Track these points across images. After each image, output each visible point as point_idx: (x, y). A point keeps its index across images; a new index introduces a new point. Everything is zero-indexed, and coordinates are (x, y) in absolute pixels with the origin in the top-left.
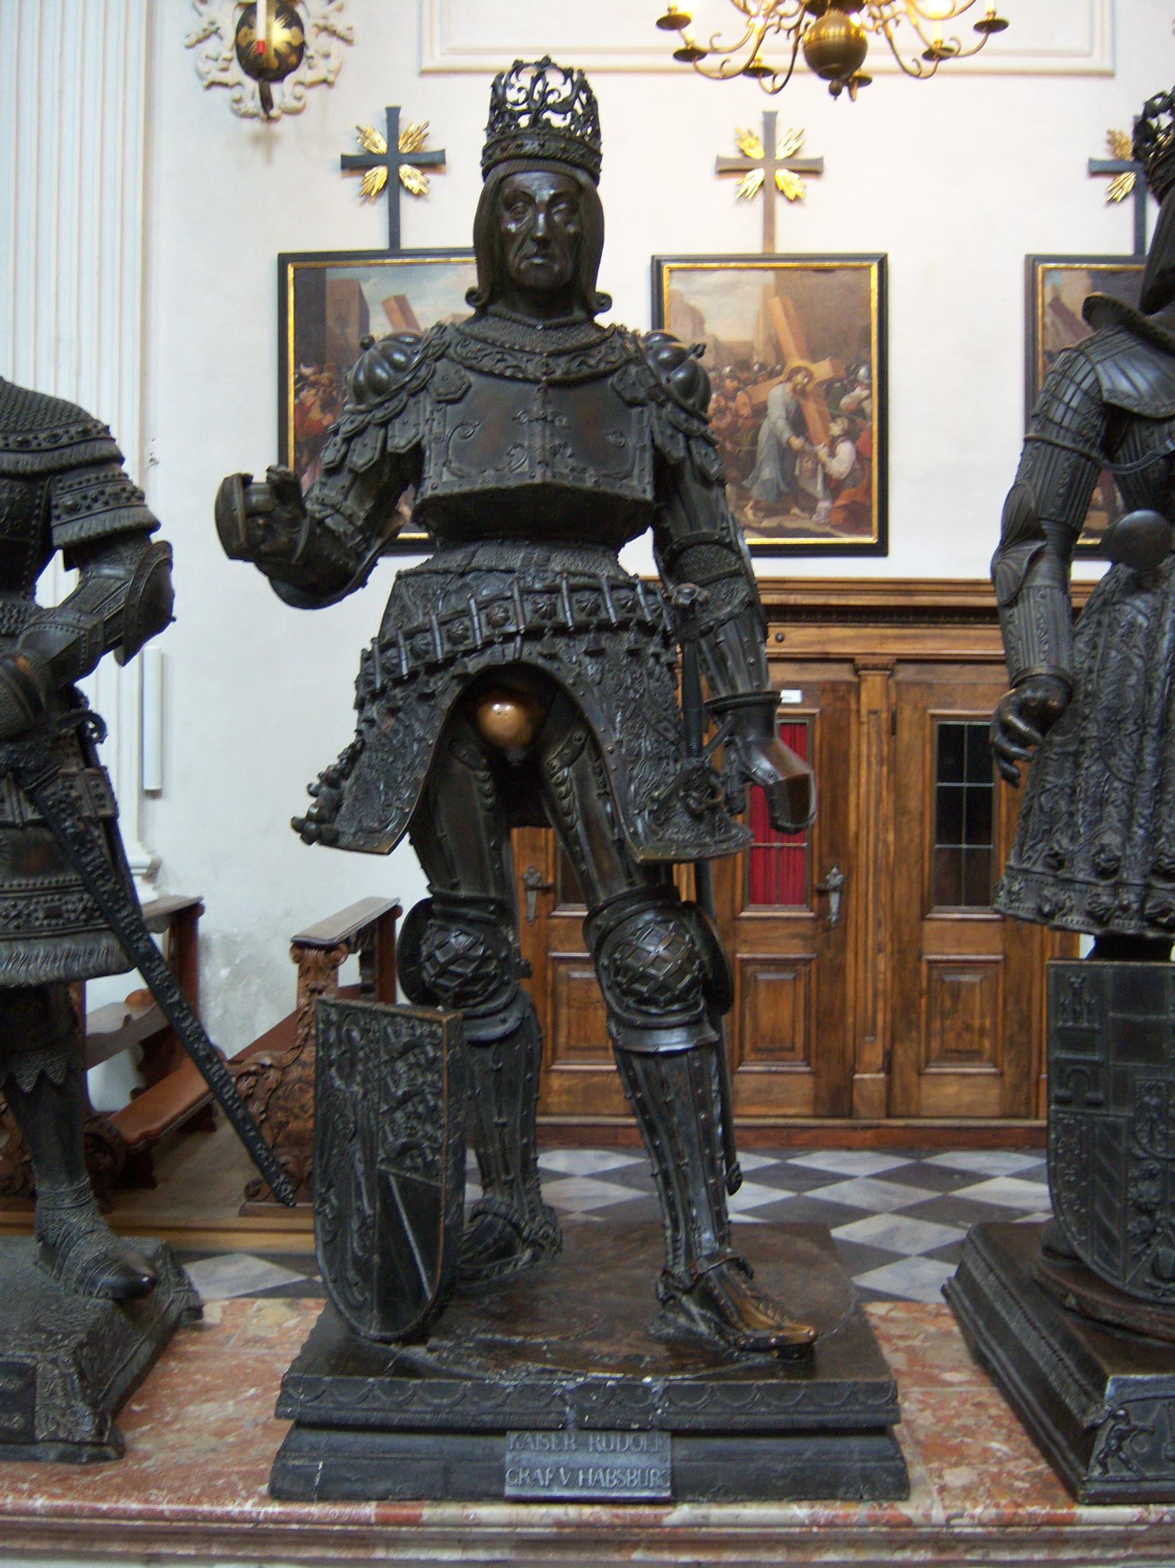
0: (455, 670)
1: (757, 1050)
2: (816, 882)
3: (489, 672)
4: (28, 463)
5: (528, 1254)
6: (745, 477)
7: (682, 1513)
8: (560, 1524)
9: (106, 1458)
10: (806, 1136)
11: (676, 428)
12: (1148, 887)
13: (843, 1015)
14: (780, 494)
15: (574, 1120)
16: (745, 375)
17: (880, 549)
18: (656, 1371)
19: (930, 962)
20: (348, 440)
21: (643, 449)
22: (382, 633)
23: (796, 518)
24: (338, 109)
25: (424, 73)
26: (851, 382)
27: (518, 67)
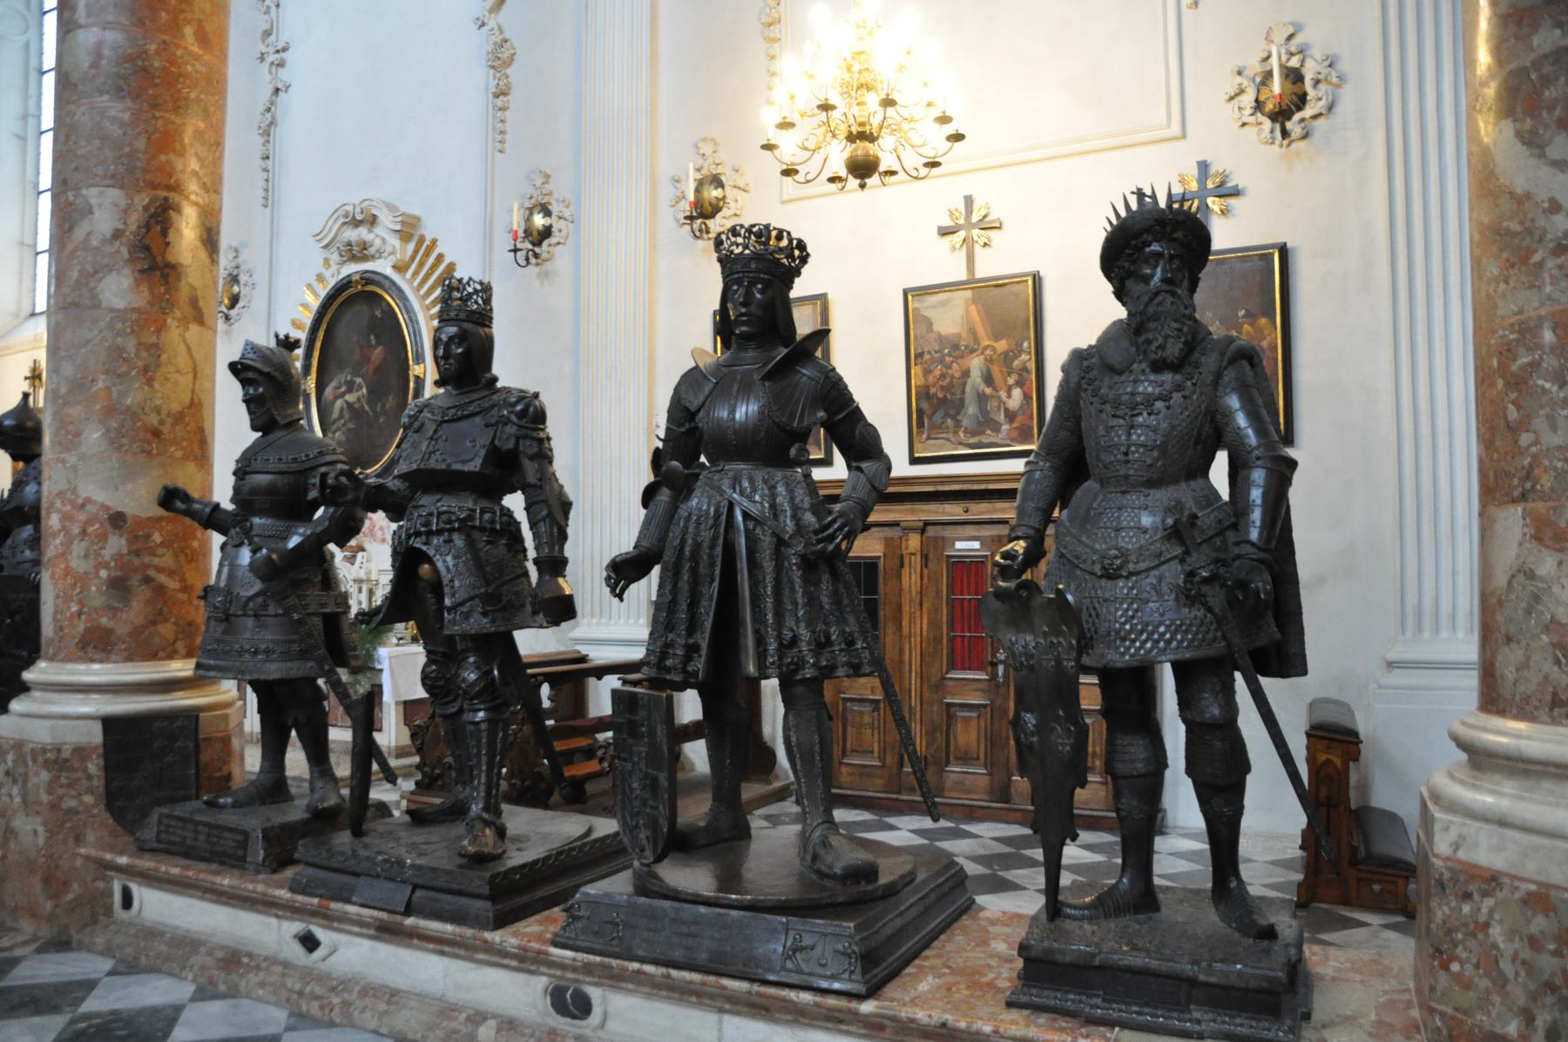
1: (957, 758)
4: (295, 467)
6: (958, 413)
14: (979, 422)
23: (989, 436)
25: (783, 202)
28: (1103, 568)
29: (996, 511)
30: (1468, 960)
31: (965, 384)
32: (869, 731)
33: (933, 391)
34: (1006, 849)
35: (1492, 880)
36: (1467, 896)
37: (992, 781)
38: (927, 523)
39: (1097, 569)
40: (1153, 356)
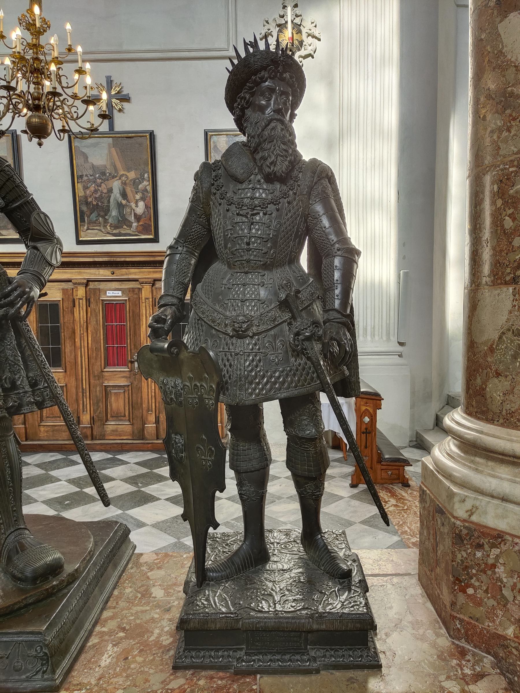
1: (112, 417)
2: (129, 359)
6: (106, 215)
10: (128, 446)
13: (142, 404)
14: (119, 221)
15: (46, 443)
16: (104, 178)
17: (156, 240)
23: (125, 230)
28: (234, 330)
29: (131, 274)
30: (480, 587)
33: (90, 200)
34: (145, 470)
35: (498, 537)
36: (480, 546)
37: (133, 428)
38: (89, 281)
39: (229, 330)
40: (267, 170)
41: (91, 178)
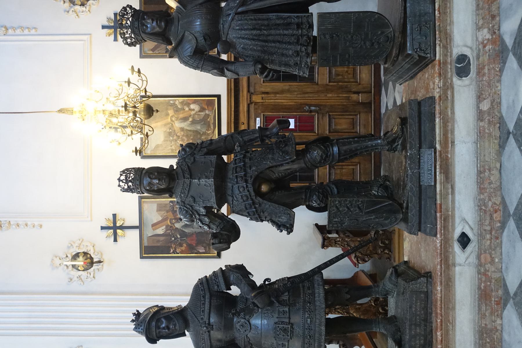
0: (254, 198)
1: (353, 128)
3: (254, 191)
4: (208, 296)
5: (388, 183)
6: (200, 133)
7: (438, 147)
8: (440, 173)
9: (431, 275)
11: (199, 151)
12: (301, 44)
13: (343, 105)
17: (219, 97)
18: (407, 152)
19: (329, 82)
20: (203, 224)
21: (205, 158)
22: (246, 216)
23: (211, 120)
24: (100, 243)
26: (174, 105)
27: (119, 186)
29: (243, 109)
31: (187, 130)
32: (344, 170)
41: (173, 143)
